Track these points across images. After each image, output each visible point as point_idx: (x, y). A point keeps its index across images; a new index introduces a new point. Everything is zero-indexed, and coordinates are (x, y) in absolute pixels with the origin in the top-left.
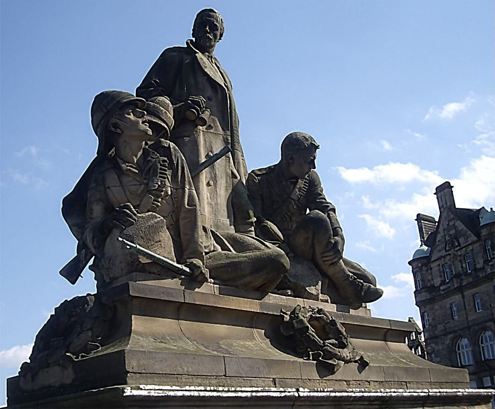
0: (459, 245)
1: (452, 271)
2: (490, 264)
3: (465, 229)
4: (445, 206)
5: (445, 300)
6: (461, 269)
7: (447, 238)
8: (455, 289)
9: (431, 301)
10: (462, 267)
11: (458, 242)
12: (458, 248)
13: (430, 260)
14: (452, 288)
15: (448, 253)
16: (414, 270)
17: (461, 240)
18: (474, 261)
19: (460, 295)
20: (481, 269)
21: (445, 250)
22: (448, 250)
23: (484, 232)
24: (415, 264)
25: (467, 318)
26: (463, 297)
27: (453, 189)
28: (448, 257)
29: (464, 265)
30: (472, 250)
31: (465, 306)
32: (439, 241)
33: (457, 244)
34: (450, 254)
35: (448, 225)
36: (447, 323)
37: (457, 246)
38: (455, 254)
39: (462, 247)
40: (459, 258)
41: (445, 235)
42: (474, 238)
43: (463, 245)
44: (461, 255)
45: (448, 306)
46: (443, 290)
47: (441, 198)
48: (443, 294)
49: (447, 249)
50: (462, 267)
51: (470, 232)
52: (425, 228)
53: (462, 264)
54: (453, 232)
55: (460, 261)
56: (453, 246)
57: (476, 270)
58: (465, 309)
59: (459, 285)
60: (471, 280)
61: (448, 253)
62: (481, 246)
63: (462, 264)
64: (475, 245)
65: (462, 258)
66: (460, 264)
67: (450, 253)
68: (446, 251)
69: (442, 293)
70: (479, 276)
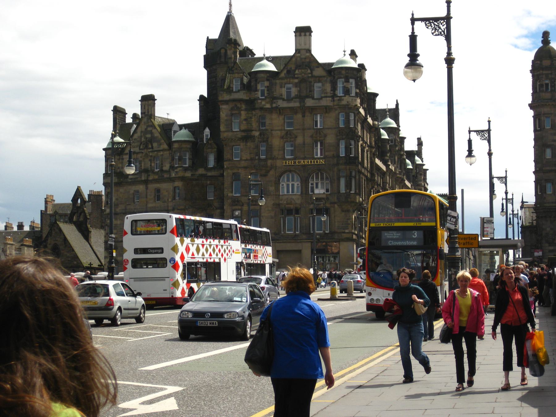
0: (152, 148)
1: (141, 166)
2: (175, 170)
3: (160, 137)
4: (146, 113)
5: (130, 187)
6: (149, 167)
7: (143, 139)
8: (142, 181)
9: (118, 184)
10: (151, 165)
11: (152, 145)
12: (151, 150)
13: (124, 152)
14: (139, 179)
15: (141, 151)
16: (107, 157)
17: (155, 145)
18: (162, 164)
19: (144, 186)
20: (166, 171)
21: (139, 148)
22: (142, 149)
23: (176, 146)
24: (110, 152)
25: (147, 205)
26: (147, 188)
27: (156, 101)
28: (140, 155)
29: (153, 164)
30: (163, 155)
31: (147, 195)
32: (135, 139)
33: (150, 146)
34: (142, 153)
35: (146, 129)
36: (128, 205)
37: (150, 148)
38: (146, 154)
39: (154, 150)
40: (149, 158)
41: (141, 137)
42: (165, 146)
43: (155, 149)
44: (151, 156)
45: (132, 192)
46: (131, 179)
47: (145, 106)
48: (130, 182)
49: (141, 147)
50: (151, 165)
51: (163, 141)
52: (118, 119)
53: (151, 163)
54: (149, 136)
55: (150, 160)
56: (146, 147)
57: (162, 170)
58: (147, 197)
59: (146, 178)
60: (156, 177)
61: (141, 151)
62: (170, 155)
63: (151, 163)
64: (165, 152)
65: (152, 159)
66: (149, 162)
67: (143, 151)
68: (140, 149)
69: (130, 181)
70: (163, 176)
